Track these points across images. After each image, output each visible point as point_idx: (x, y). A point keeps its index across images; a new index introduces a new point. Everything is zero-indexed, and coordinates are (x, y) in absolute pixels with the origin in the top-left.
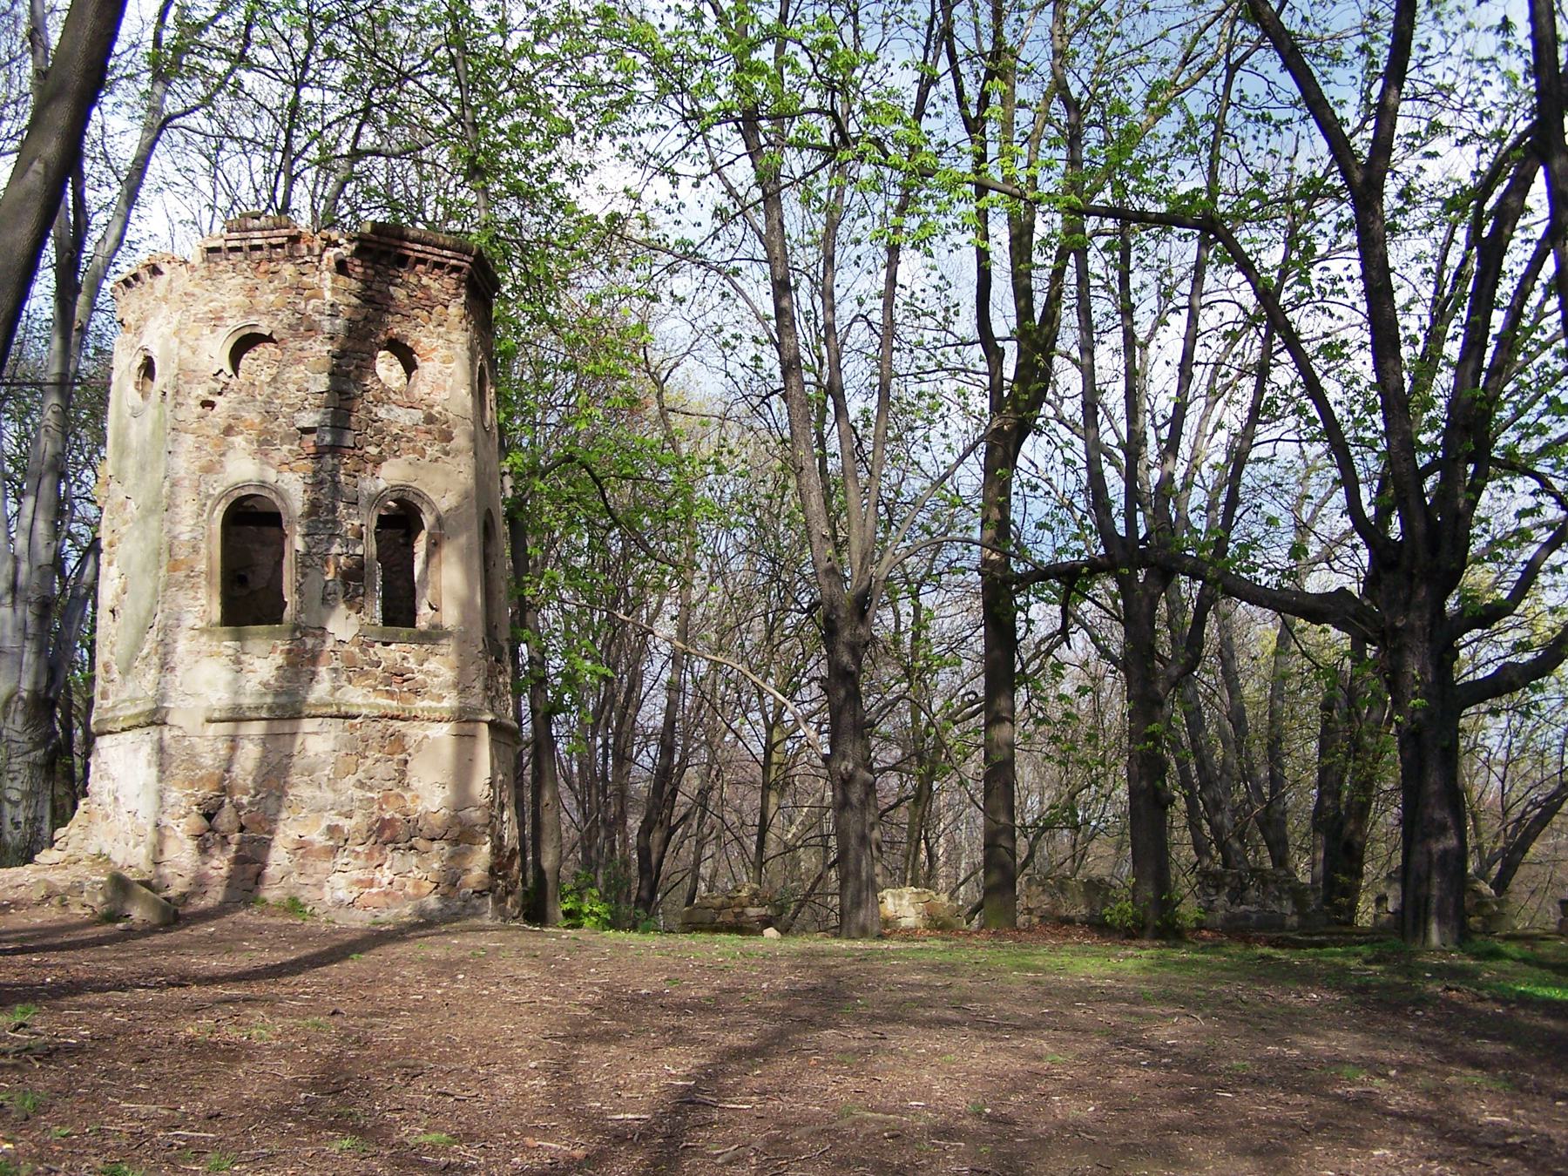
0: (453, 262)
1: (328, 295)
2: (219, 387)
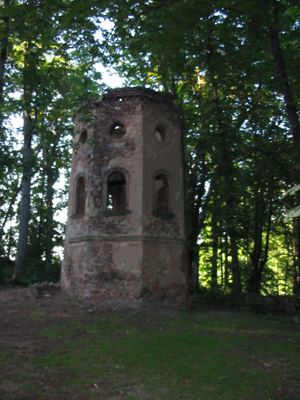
0: (136, 94)
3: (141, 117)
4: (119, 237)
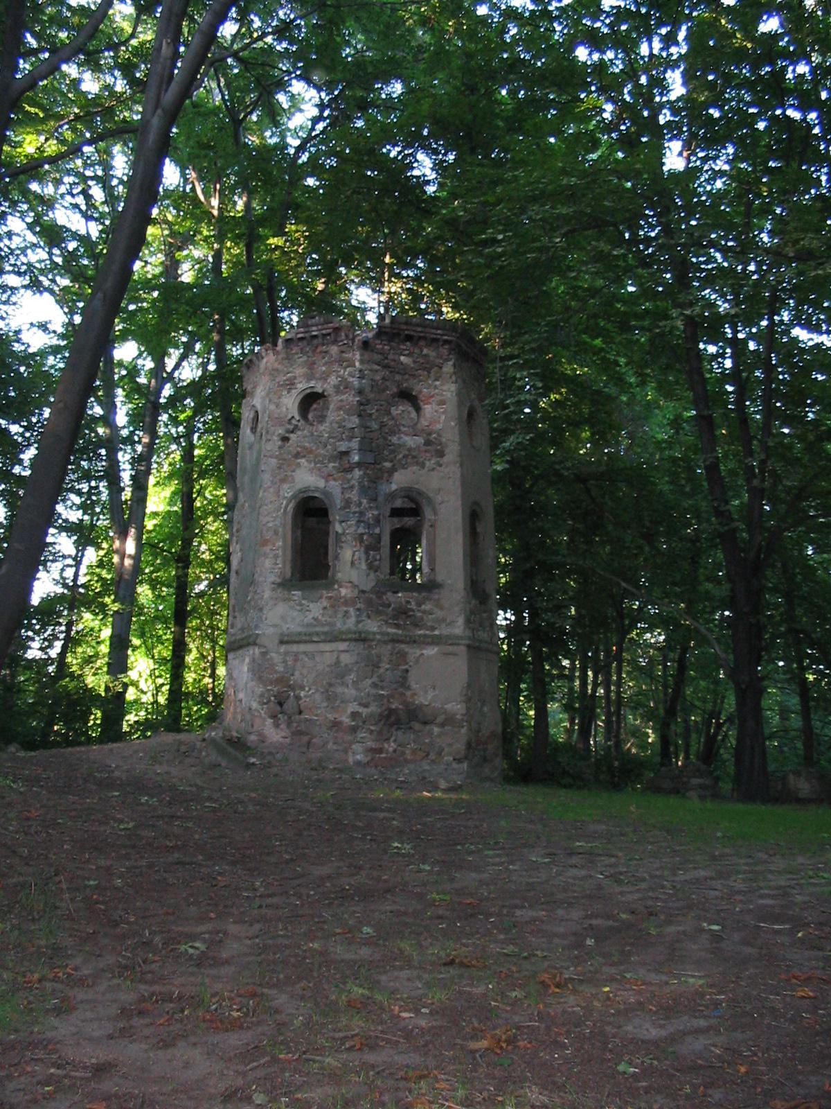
0: (446, 337)
1: (357, 364)
2: (291, 427)
3: (453, 387)
4: (420, 636)
